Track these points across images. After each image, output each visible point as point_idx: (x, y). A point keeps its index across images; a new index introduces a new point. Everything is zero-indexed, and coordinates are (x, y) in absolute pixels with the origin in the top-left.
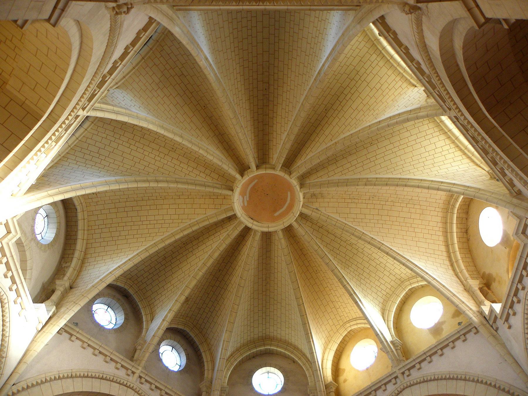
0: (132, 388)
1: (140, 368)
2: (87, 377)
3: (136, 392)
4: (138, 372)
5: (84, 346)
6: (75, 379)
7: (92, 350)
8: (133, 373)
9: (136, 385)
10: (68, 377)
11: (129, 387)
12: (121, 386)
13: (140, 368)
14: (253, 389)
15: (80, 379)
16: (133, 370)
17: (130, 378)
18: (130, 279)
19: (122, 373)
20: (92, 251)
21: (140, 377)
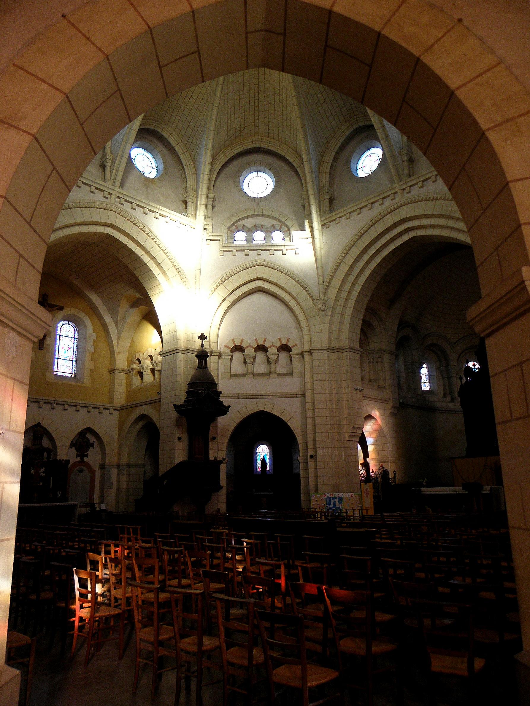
0: (402, 206)
1: (396, 185)
2: (363, 234)
3: (407, 204)
8: (396, 193)
10: (351, 248)
11: (398, 208)
13: (396, 185)
16: (393, 191)
17: (397, 199)
18: (350, 118)
21: (404, 189)
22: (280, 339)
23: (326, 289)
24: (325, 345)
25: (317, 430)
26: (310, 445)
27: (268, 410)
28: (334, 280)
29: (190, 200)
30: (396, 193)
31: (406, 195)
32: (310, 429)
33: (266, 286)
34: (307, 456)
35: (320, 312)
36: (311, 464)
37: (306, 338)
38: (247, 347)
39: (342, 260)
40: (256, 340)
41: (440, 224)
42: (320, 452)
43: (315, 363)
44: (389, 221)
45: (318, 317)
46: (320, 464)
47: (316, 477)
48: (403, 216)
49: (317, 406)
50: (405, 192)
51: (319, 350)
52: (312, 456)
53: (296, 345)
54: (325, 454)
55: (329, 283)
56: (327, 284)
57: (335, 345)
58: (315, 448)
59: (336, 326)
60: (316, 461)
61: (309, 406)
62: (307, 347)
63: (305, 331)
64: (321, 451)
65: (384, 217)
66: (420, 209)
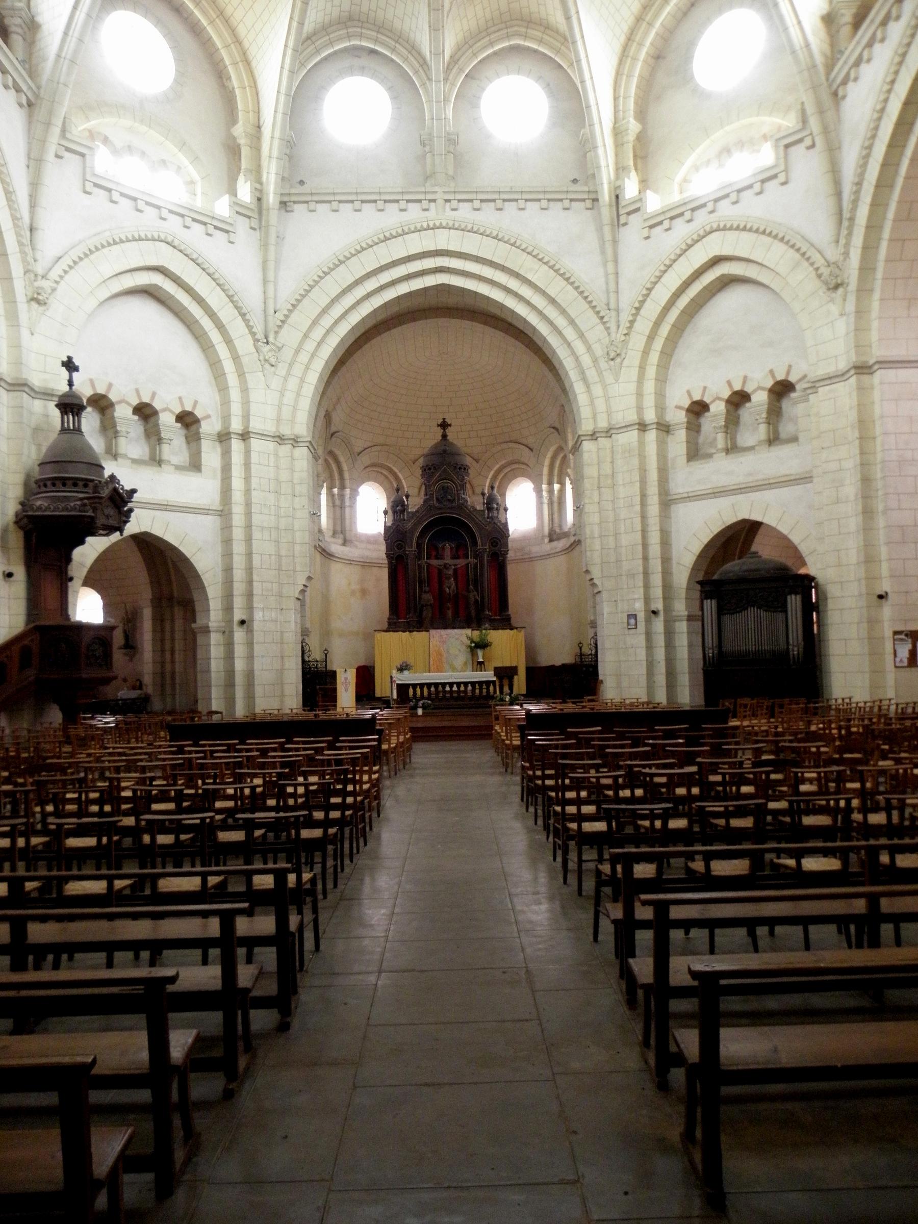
0: (441, 227)
2: (363, 249)
3: (450, 228)
4: (440, 197)
5: (335, 208)
6: (348, 262)
7: (350, 205)
8: (434, 201)
9: (448, 216)
11: (434, 228)
12: (423, 233)
14: (696, 90)
15: (354, 259)
16: (429, 197)
19: (414, 214)
20: (242, 31)
21: (447, 201)
22: (180, 398)
23: (280, 327)
24: (270, 428)
25: (255, 578)
26: (239, 602)
27: (157, 531)
28: (296, 312)
29: (19, 30)
30: (434, 201)
31: (449, 213)
32: (239, 574)
33: (168, 286)
34: (230, 621)
35: (267, 366)
36: (239, 635)
37: (236, 409)
38: (120, 402)
39: (317, 282)
40: (137, 391)
41: (496, 279)
42: (258, 615)
43: (254, 458)
44: (416, 243)
45: (260, 374)
46: (258, 637)
47: (250, 657)
48: (442, 246)
49: (256, 535)
50: (448, 204)
51: (263, 436)
52: (243, 622)
53: (208, 417)
54: (266, 618)
55: (287, 316)
56: (282, 318)
57: (286, 431)
58: (250, 608)
59: (289, 397)
60: (250, 631)
61: (238, 533)
62: (236, 426)
63: (235, 394)
64: (261, 614)
65: (407, 233)
66: (470, 244)
